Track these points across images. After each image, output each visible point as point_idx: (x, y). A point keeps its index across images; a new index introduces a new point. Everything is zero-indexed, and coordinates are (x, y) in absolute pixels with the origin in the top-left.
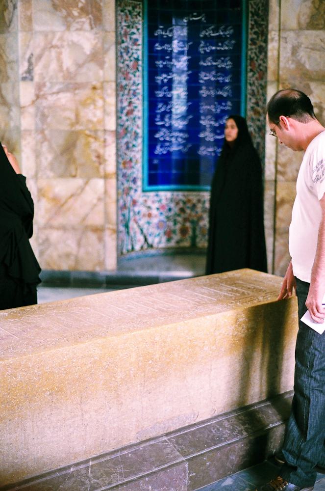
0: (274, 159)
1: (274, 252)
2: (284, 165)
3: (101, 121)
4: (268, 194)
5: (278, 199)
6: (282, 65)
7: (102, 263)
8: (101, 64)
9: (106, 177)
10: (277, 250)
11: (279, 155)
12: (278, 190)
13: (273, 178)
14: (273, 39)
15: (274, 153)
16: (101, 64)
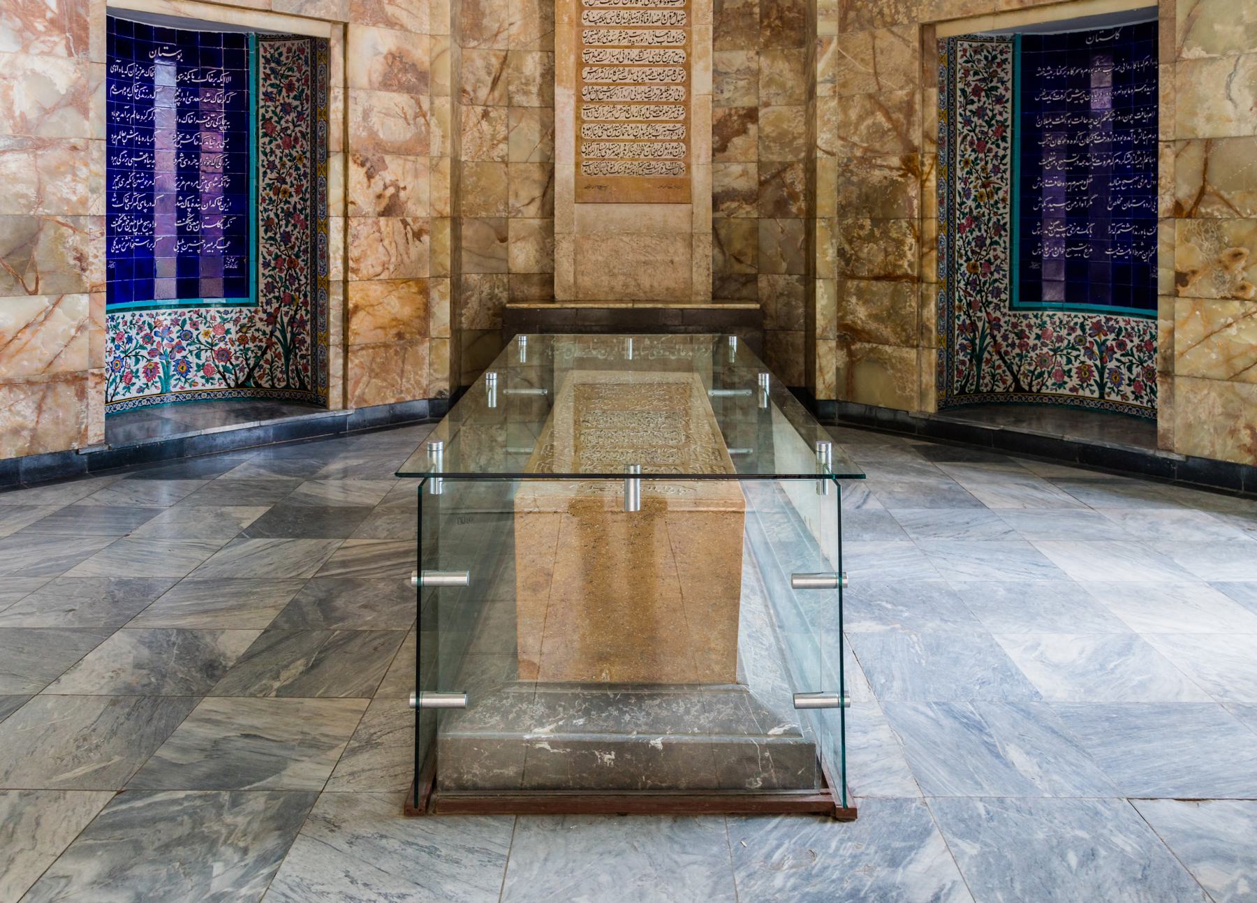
0: (341, 252)
1: (345, 378)
2: (357, 260)
3: (83, 202)
4: (335, 300)
5: (351, 305)
6: (351, 131)
7: (82, 435)
8: (85, 112)
9: (92, 291)
10: (351, 374)
11: (350, 248)
12: (351, 294)
13: (341, 278)
14: (336, 98)
15: (341, 246)
16: (85, 112)
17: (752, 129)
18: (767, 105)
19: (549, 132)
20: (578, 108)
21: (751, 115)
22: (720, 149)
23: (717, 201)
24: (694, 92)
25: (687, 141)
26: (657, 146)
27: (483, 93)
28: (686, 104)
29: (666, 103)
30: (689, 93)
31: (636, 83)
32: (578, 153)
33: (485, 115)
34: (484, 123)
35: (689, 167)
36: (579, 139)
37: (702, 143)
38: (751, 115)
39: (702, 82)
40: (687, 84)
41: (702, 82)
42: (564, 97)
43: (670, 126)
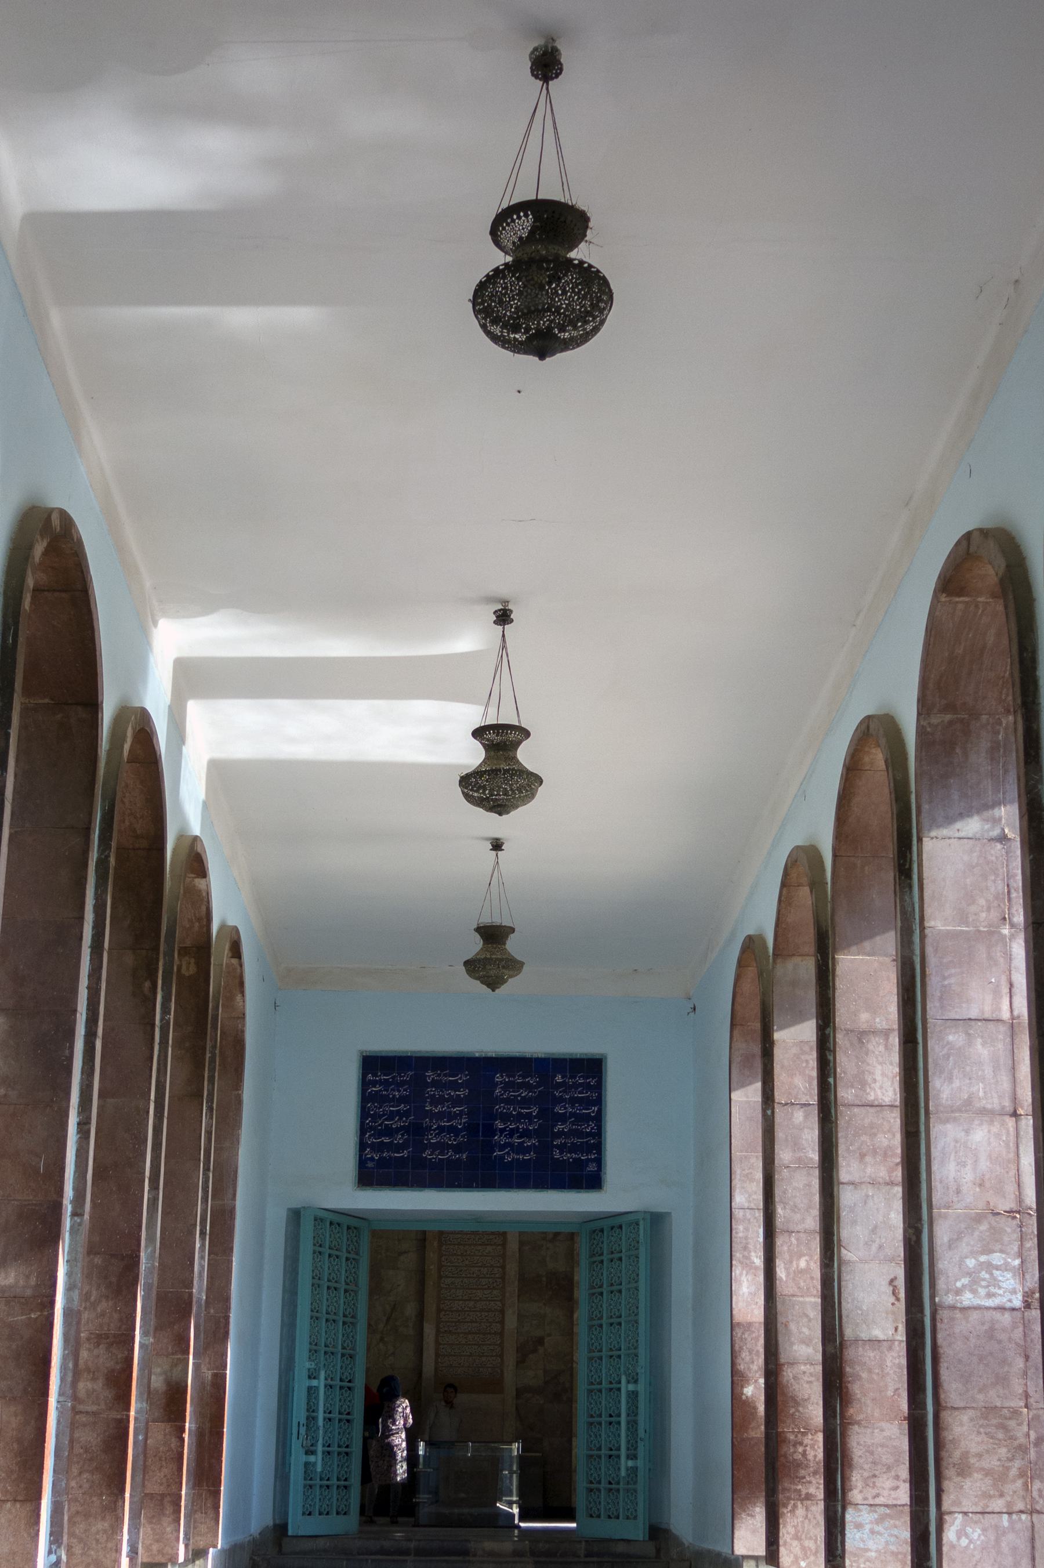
17: (541, 1350)
18: (549, 1335)
19: (420, 1351)
20: (437, 1336)
21: (540, 1341)
22: (521, 1362)
23: (519, 1393)
24: (506, 1327)
25: (501, 1356)
26: (484, 1359)
27: (381, 1326)
28: (501, 1334)
29: (490, 1333)
30: (503, 1328)
31: (472, 1322)
32: (436, 1362)
33: (382, 1339)
34: (381, 1344)
35: (502, 1371)
36: (437, 1355)
37: (511, 1359)
38: (540, 1341)
39: (511, 1322)
40: (502, 1322)
41: (511, 1322)
42: (429, 1331)
43: (491, 1347)
